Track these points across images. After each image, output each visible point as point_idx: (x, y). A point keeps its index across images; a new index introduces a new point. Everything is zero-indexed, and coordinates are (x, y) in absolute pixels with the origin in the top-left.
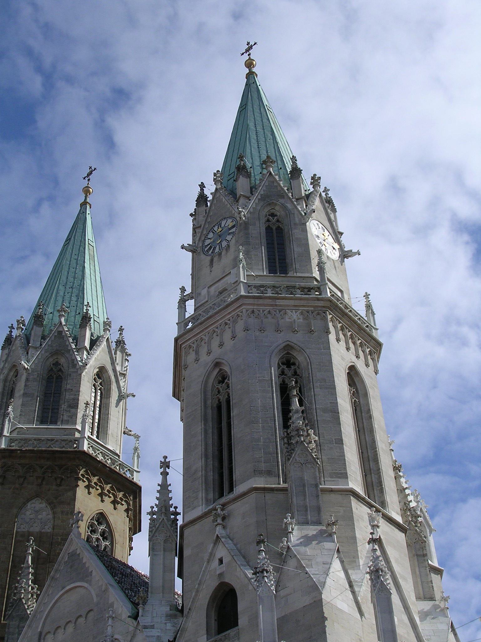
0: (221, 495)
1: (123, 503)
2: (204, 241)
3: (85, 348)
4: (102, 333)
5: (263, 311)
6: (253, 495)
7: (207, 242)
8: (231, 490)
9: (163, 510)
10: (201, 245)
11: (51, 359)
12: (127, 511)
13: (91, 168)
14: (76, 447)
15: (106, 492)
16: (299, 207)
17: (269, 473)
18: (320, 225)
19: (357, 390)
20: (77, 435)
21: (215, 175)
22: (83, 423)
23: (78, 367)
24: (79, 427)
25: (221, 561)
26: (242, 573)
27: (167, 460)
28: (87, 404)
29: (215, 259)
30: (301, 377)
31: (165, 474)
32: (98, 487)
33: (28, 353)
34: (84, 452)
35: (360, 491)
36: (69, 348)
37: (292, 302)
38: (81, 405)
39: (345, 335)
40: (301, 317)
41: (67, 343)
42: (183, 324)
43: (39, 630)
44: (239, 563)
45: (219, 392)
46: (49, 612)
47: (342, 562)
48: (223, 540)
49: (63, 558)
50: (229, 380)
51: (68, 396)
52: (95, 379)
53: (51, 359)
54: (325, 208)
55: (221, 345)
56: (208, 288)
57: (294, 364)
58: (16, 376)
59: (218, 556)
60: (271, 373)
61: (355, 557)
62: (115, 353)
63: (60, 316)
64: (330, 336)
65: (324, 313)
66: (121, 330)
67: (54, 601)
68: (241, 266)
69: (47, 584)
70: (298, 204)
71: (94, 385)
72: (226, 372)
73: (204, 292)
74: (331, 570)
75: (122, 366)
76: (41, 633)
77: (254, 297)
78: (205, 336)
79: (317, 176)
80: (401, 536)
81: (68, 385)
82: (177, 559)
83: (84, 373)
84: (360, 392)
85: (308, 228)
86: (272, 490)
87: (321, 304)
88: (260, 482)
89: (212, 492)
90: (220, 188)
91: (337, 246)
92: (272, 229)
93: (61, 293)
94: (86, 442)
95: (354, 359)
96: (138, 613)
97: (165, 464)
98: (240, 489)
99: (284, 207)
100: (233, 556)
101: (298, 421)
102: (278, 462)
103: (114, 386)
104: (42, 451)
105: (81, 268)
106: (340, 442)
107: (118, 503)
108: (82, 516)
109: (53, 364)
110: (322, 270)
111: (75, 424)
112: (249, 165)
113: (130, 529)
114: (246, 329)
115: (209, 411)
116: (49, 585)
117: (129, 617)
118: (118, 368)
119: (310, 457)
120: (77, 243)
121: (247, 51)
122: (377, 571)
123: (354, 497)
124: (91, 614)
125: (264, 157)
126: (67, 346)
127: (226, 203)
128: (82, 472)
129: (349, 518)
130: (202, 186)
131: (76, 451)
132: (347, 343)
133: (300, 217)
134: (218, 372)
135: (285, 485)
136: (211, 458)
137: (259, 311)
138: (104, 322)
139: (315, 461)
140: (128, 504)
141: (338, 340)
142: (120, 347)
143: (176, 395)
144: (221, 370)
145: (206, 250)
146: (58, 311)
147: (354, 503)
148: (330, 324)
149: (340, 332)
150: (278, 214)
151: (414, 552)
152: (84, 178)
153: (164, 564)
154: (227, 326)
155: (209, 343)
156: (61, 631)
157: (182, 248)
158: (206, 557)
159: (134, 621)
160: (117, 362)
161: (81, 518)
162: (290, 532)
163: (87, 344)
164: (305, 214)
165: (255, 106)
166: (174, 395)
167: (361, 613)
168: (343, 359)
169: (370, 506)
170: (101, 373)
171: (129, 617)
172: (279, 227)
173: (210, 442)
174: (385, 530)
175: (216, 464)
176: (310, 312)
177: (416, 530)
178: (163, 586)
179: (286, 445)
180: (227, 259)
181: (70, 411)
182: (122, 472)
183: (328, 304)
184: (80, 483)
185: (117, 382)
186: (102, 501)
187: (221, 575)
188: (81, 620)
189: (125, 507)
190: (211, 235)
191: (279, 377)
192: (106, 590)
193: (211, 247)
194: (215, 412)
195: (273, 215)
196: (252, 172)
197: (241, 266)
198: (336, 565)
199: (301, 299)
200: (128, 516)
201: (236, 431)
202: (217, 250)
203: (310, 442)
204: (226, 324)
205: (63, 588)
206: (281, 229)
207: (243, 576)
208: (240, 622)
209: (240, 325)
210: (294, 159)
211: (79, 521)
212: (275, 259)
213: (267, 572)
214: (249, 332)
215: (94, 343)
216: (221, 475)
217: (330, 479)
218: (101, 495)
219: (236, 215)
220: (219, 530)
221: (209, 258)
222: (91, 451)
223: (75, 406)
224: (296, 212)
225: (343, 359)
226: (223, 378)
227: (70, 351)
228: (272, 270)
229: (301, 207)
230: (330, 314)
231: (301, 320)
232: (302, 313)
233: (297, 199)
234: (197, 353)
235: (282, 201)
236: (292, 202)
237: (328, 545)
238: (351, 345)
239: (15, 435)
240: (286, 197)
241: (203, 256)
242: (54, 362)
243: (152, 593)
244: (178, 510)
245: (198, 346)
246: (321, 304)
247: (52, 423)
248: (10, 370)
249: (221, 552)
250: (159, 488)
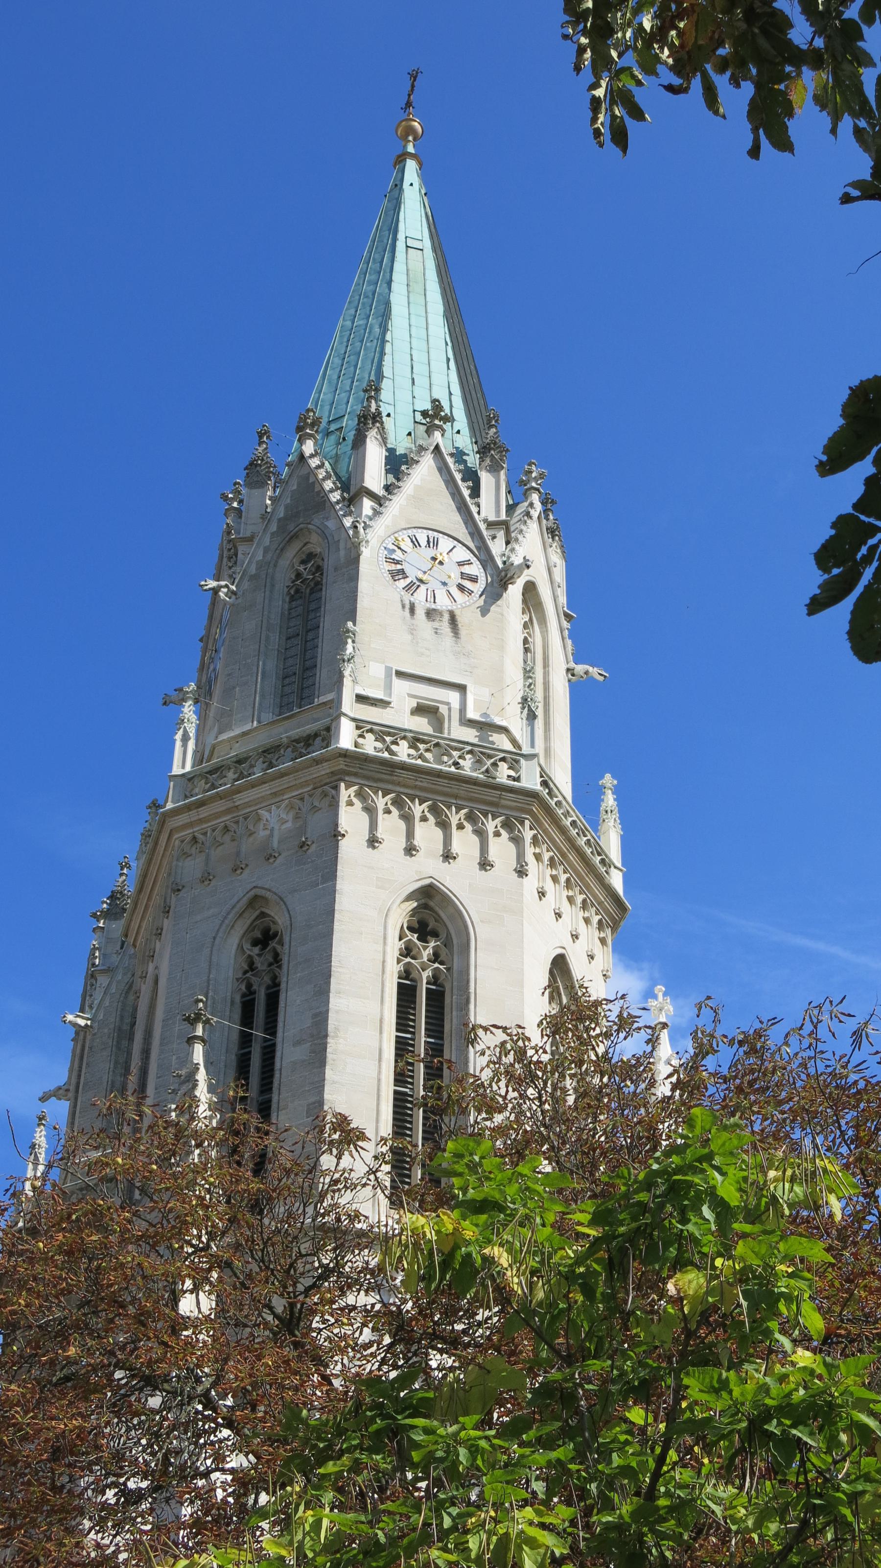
37: (264, 790)
64: (343, 844)
87: (324, 769)
91: (475, 569)
99: (323, 534)
157: (165, 704)
183: (341, 764)
197: (179, 736)
214: (181, 894)
232: (291, 807)
246: (324, 769)
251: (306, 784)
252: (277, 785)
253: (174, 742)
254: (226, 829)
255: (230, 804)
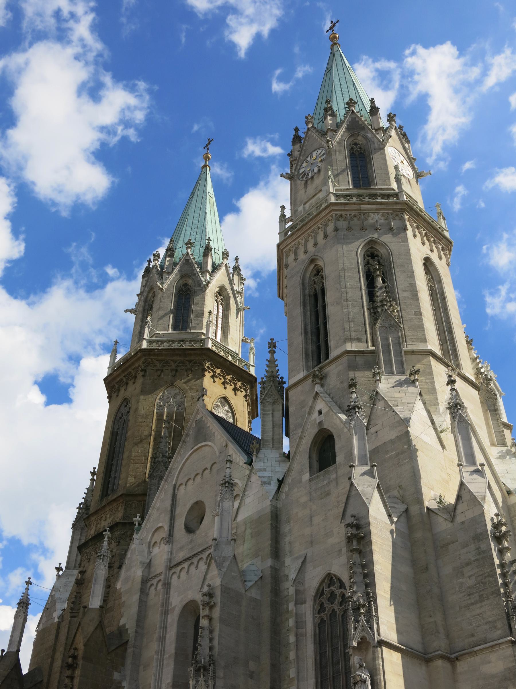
0: (319, 362)
1: (242, 390)
2: (299, 170)
3: (208, 271)
4: (221, 260)
5: (350, 215)
6: (345, 358)
7: (302, 170)
8: (327, 357)
9: (271, 379)
10: (297, 173)
11: (181, 282)
12: (245, 396)
13: (209, 139)
14: (202, 346)
15: (228, 381)
16: (377, 136)
17: (359, 340)
18: (397, 151)
19: (432, 277)
20: (203, 337)
21: (307, 117)
22: (208, 326)
23: (202, 286)
24: (204, 331)
25: (320, 413)
26: (338, 420)
27: (274, 341)
28: (210, 313)
29: (309, 182)
30: (383, 266)
31: (272, 352)
32: (221, 377)
33: (162, 278)
34: (209, 349)
35: (438, 351)
36: (195, 272)
37: (374, 207)
38: (206, 314)
39: (420, 233)
40: (383, 218)
41: (193, 268)
42: (283, 233)
43: (174, 483)
44: (335, 411)
45: (315, 283)
46: (181, 468)
47: (424, 404)
48: (321, 395)
49: (191, 425)
50: (322, 272)
51: (195, 308)
52: (216, 296)
53: (181, 282)
54: (400, 139)
55: (315, 245)
56: (304, 205)
57: (377, 256)
58: (154, 297)
59: (317, 408)
60: (358, 263)
61: (436, 403)
62: (233, 276)
63: (187, 248)
64: (407, 232)
65: (402, 214)
66: (237, 259)
67: (185, 459)
68: (330, 180)
69: (180, 445)
70: (378, 134)
71: (216, 301)
72: (320, 266)
73: (301, 208)
74: (415, 409)
75: (239, 287)
76: (175, 486)
77: (341, 204)
78: (302, 240)
79: (393, 114)
80: (475, 393)
81: (196, 300)
82: (284, 419)
83: (207, 291)
84: (434, 279)
85: (386, 152)
86: (362, 353)
87: (399, 207)
88: (351, 347)
89: (311, 361)
90: (311, 127)
92: (355, 155)
93: (188, 233)
94: (210, 342)
95: (429, 252)
96: (252, 460)
97: (272, 345)
98: (333, 354)
99: (366, 138)
100: (330, 407)
101: (380, 294)
102: (366, 331)
103: (232, 302)
104: (174, 349)
105: (204, 213)
106: (419, 313)
107: (238, 390)
108: (206, 391)
109: (183, 285)
110: (398, 180)
111: (202, 329)
112: (335, 108)
113: (249, 412)
114: (336, 229)
115: (308, 298)
116: (181, 447)
117: (245, 463)
118: (236, 288)
119: (393, 322)
120: (200, 195)
121: (331, 28)
122: (456, 406)
123: (433, 357)
124: (215, 466)
125: (347, 100)
126: (194, 270)
127: (317, 137)
128: (207, 365)
129: (430, 373)
130: (297, 130)
131: (203, 349)
132: (422, 239)
133: (379, 143)
134: (314, 267)
135: (373, 348)
136: (310, 335)
137: (347, 215)
138: (223, 253)
139: (398, 324)
140: (246, 391)
141: (415, 236)
142: (236, 272)
143: (281, 296)
144: (316, 265)
145: (301, 176)
146: (186, 244)
147: (433, 361)
148: (408, 224)
149: (417, 231)
150: (361, 143)
151: (486, 408)
152: (204, 148)
153: (273, 421)
154: (320, 230)
155: (305, 245)
156: (190, 482)
157: (281, 176)
158: (307, 410)
159: (249, 467)
160: (234, 283)
161: (205, 393)
162: (378, 380)
163: (210, 268)
164: (383, 141)
165: (339, 68)
166: (279, 296)
167: (443, 447)
168: (419, 251)
169: (447, 366)
170: (221, 291)
171: (245, 463)
172: (361, 153)
173: (309, 321)
174: (460, 385)
175: (314, 338)
176: (390, 214)
177: (488, 390)
178: (273, 439)
179: (372, 315)
180: (318, 181)
181: (197, 320)
182: (240, 366)
183: (405, 207)
184: (206, 373)
185: (235, 298)
186: (225, 388)
187: (320, 423)
188: (207, 472)
189: (244, 393)
190: (305, 165)
191: (365, 266)
192: (226, 446)
193: (305, 174)
194: (313, 299)
195: (356, 144)
196: (338, 113)
197: (330, 180)
198: (419, 405)
199: (381, 203)
200: (246, 401)
201: (331, 309)
202: (310, 175)
203: (393, 311)
204: (319, 228)
205: (193, 448)
206: (364, 155)
207: (338, 422)
208: (338, 459)
209: (330, 228)
210: (372, 101)
211: (203, 395)
212: (359, 178)
213: (359, 409)
214: (338, 232)
215: (216, 268)
216: (319, 347)
217: (411, 343)
218: (224, 383)
219: (325, 145)
220: (318, 388)
221: (303, 182)
222: (214, 349)
223: (201, 314)
224: (375, 140)
225: (419, 251)
226: (318, 272)
227: (195, 274)
228: (356, 184)
229: (380, 136)
230: (407, 215)
231: (382, 221)
232: (383, 216)
233: (376, 130)
234: (296, 254)
235: (362, 133)
236: (372, 132)
237: (411, 389)
238: (426, 241)
239: (154, 338)
240: (366, 129)
241: (298, 182)
242: (184, 283)
243: (263, 444)
244: (284, 380)
245: (297, 249)
247: (182, 330)
248: (149, 292)
249: (320, 405)
250: (268, 363)
251: (390, 209)
252: (379, 207)
253: (329, 182)
254: (355, 216)
255: (358, 208)
